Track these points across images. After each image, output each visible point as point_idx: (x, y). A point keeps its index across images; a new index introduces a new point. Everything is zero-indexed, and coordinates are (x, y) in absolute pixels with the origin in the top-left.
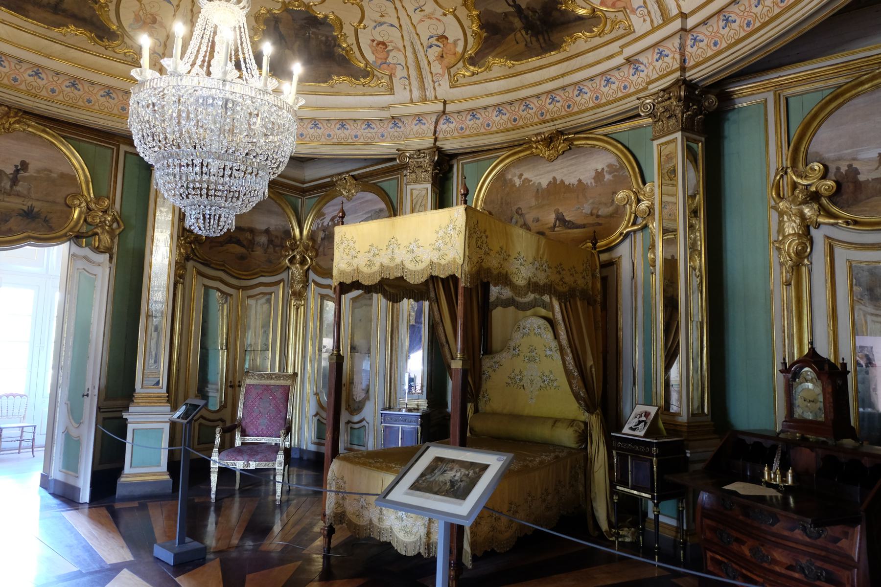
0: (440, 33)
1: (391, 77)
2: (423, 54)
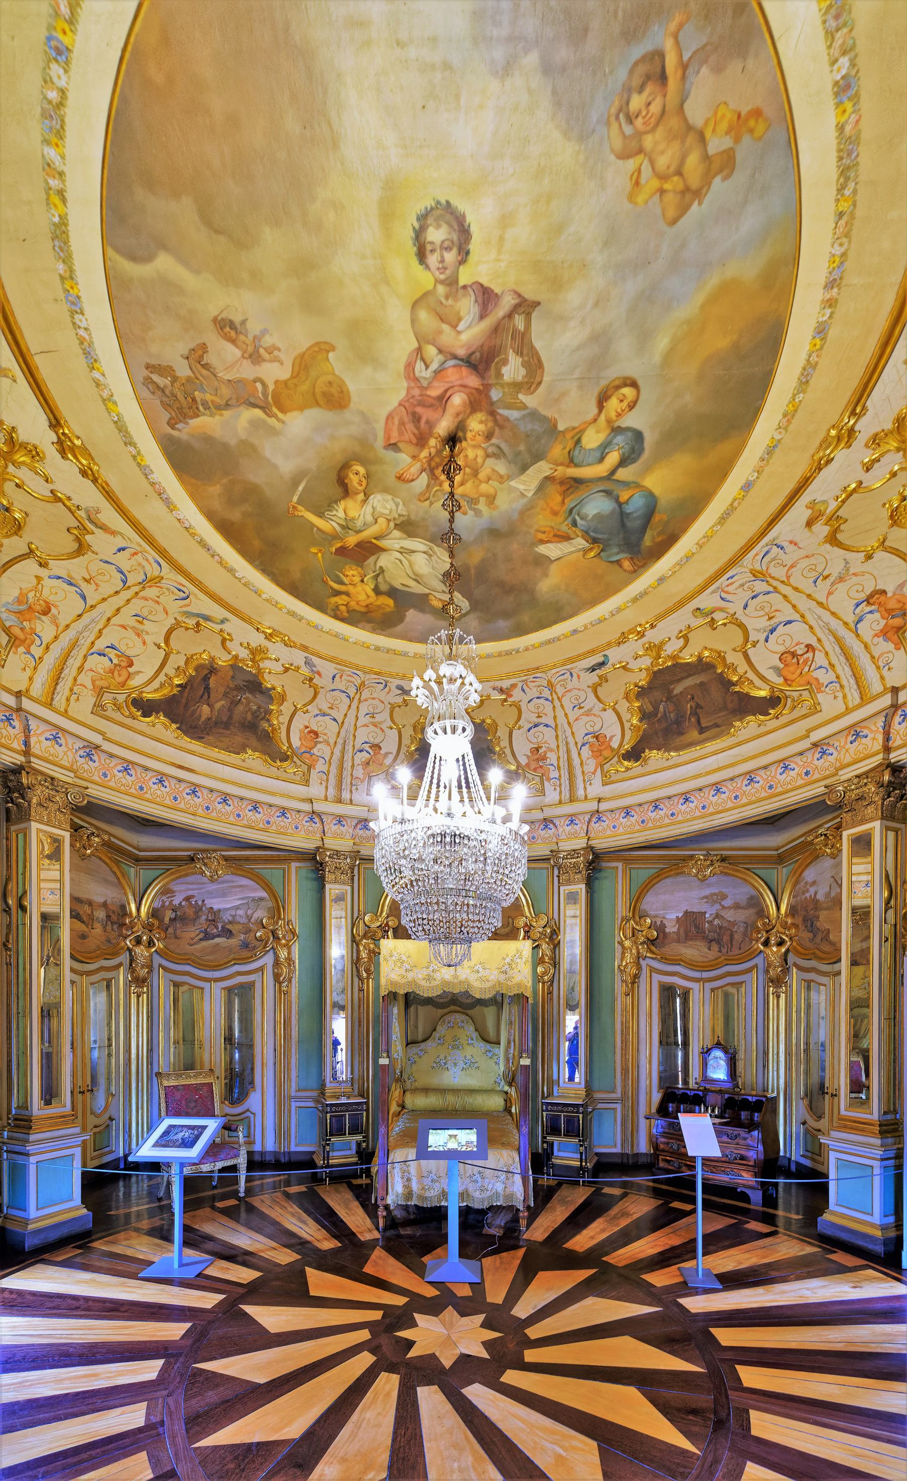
0: (376, 741)
1: (309, 768)
2: (350, 755)
